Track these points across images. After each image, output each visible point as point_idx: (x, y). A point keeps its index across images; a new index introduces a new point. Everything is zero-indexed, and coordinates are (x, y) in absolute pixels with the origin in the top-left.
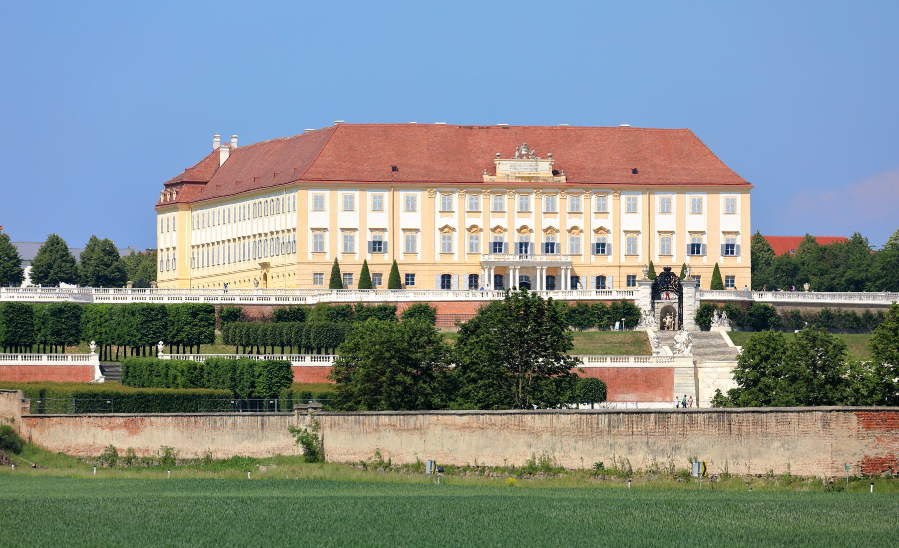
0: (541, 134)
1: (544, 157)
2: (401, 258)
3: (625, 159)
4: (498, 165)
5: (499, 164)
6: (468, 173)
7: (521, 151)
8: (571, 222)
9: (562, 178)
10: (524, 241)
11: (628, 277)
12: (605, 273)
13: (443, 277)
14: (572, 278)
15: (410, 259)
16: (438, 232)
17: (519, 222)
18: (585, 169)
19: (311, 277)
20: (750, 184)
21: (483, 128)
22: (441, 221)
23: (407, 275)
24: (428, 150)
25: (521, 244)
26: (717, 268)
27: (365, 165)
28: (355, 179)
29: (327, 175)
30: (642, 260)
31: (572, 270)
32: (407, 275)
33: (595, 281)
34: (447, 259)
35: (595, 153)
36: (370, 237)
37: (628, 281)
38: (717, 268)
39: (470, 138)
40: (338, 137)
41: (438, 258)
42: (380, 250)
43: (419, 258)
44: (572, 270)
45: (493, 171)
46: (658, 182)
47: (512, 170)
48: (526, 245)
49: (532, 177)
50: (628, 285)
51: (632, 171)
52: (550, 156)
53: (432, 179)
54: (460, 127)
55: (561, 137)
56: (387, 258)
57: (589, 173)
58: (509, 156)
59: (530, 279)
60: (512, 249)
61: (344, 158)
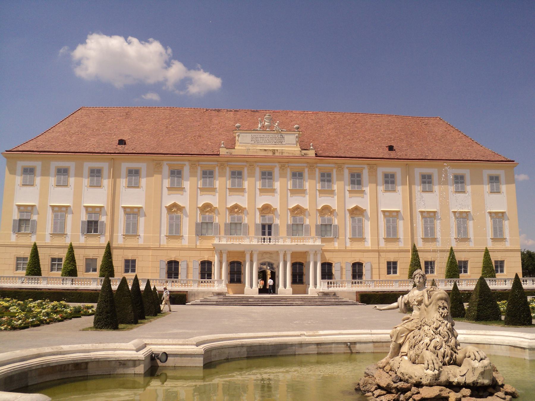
1: (290, 130)
2: (119, 240)
3: (380, 139)
4: (237, 138)
5: (238, 136)
6: (205, 147)
7: (264, 123)
8: (323, 201)
9: (311, 153)
10: (267, 222)
11: (389, 263)
12: (362, 259)
13: (170, 263)
14: (323, 265)
15: (131, 243)
16: (165, 211)
17: (262, 201)
18: (337, 145)
19: (13, 262)
20: (513, 161)
22: (169, 200)
23: (127, 261)
24: (167, 127)
25: (263, 226)
26: (487, 252)
27: (93, 139)
28: (72, 151)
29: (42, 148)
30: (405, 244)
31: (323, 256)
32: (127, 261)
33: (350, 269)
34: (175, 244)
35: (347, 133)
36: (84, 217)
37: (389, 268)
38: (487, 253)
39: (215, 118)
40: (76, 118)
41: (164, 242)
42: (96, 231)
43: (141, 242)
44: (323, 256)
46: (418, 158)
47: (253, 142)
48: (270, 227)
49: (277, 150)
50: (389, 273)
51: (387, 149)
52: (298, 128)
53: (161, 152)
56: (103, 241)
57: (341, 149)
59: (275, 266)
60: (252, 229)
61: (73, 134)
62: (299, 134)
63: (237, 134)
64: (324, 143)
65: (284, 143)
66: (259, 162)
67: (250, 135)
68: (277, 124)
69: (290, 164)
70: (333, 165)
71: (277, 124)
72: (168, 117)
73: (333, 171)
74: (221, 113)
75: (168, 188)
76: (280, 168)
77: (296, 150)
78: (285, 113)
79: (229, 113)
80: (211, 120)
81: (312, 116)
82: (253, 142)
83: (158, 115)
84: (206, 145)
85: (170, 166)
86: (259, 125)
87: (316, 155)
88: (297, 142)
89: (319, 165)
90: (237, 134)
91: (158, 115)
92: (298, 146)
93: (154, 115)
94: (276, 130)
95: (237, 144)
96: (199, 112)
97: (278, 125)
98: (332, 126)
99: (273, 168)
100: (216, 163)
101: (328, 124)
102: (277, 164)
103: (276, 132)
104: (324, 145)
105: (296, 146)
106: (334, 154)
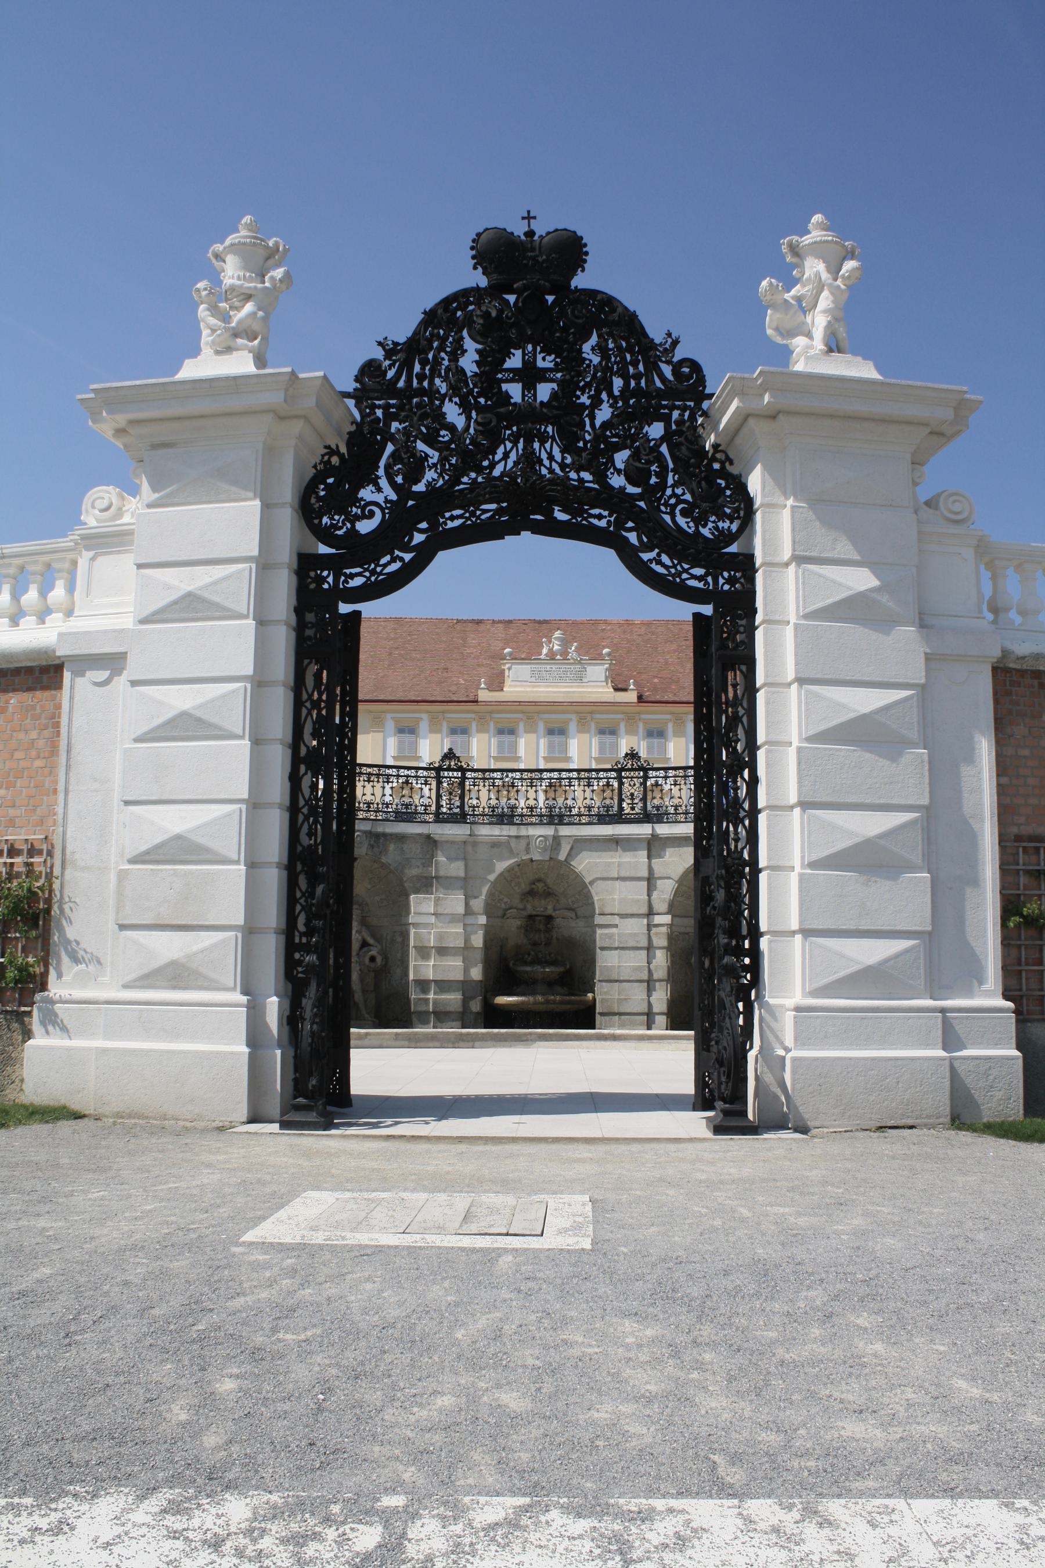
0: (603, 630)
1: (598, 658)
4: (507, 672)
5: (509, 669)
6: (454, 688)
9: (631, 696)
18: (678, 682)
21: (500, 622)
24: (390, 654)
45: (497, 683)
53: (382, 697)
54: (458, 621)
55: (640, 635)
57: (684, 688)
58: (528, 655)
62: (610, 664)
63: (507, 666)
64: (656, 677)
65: (585, 680)
66: (544, 713)
67: (529, 666)
68: (573, 648)
69: (595, 716)
70: (668, 717)
71: (573, 648)
72: (392, 635)
73: (667, 726)
74: (482, 627)
75: (393, 757)
76: (579, 722)
77: (605, 692)
78: (593, 624)
79: (496, 625)
80: (464, 640)
81: (640, 628)
82: (533, 679)
83: (374, 632)
84: (456, 685)
85: (396, 721)
86: (545, 651)
87: (640, 698)
88: (607, 678)
89: (644, 716)
90: (507, 666)
91: (374, 632)
92: (610, 684)
93: (369, 632)
94: (573, 659)
95: (508, 682)
96: (446, 626)
97: (577, 650)
98: (674, 646)
99: (567, 722)
100: (473, 716)
101: (666, 643)
102: (573, 716)
103: (572, 661)
104: (656, 680)
105: (605, 684)
106: (672, 698)
